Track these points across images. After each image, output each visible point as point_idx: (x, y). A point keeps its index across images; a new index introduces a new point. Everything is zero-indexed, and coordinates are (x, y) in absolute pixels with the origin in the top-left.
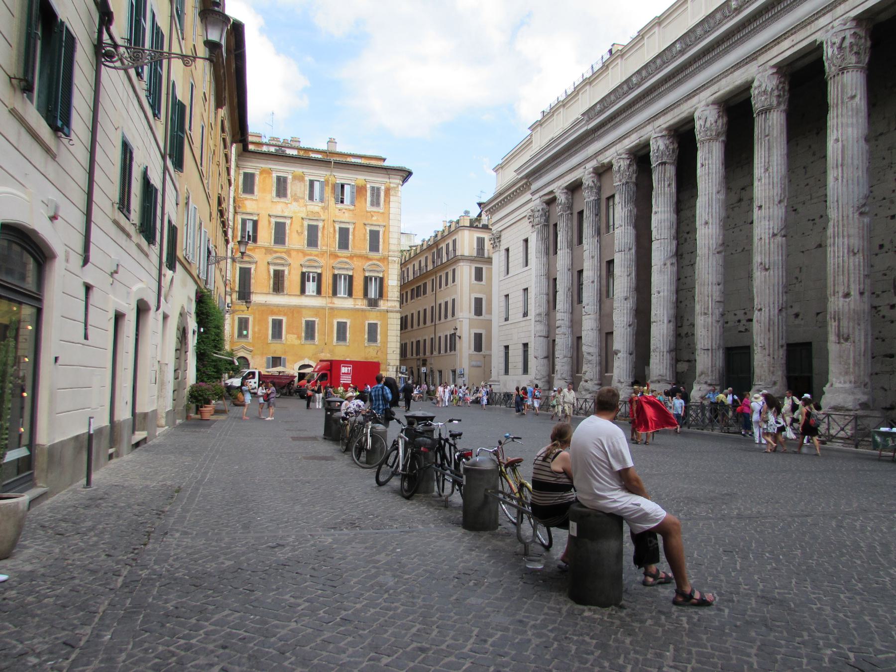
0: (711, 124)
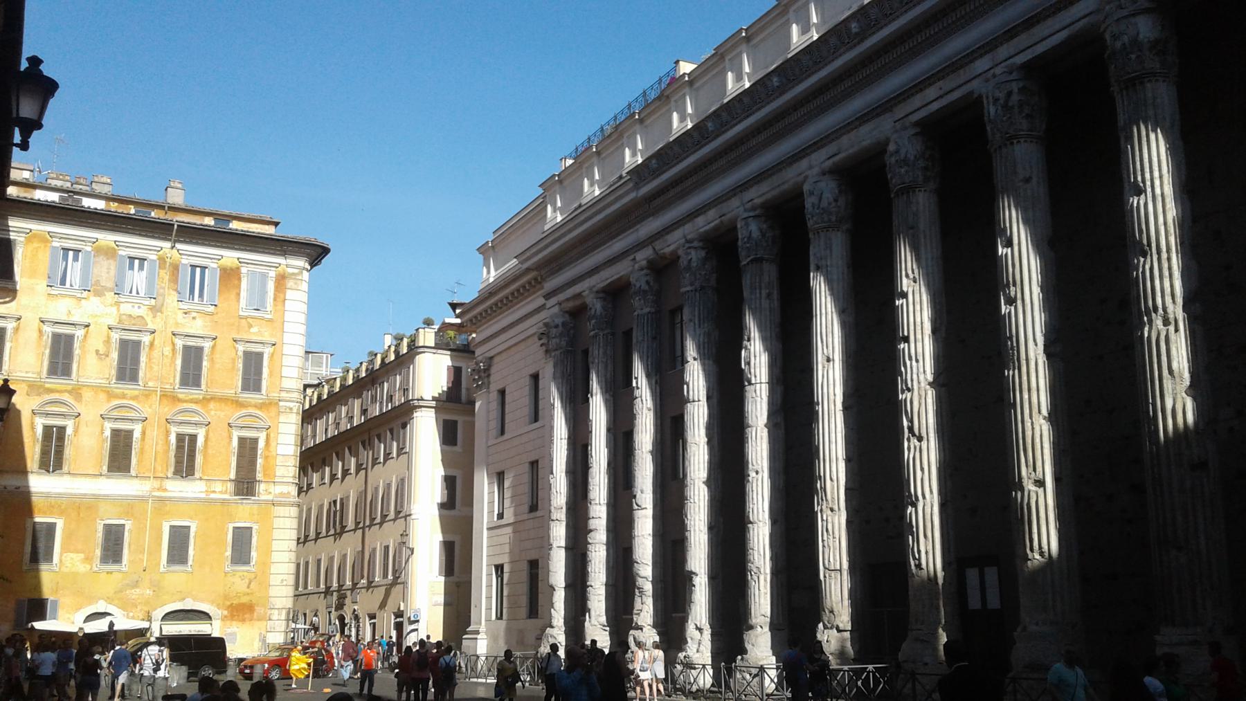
0: (830, 204)
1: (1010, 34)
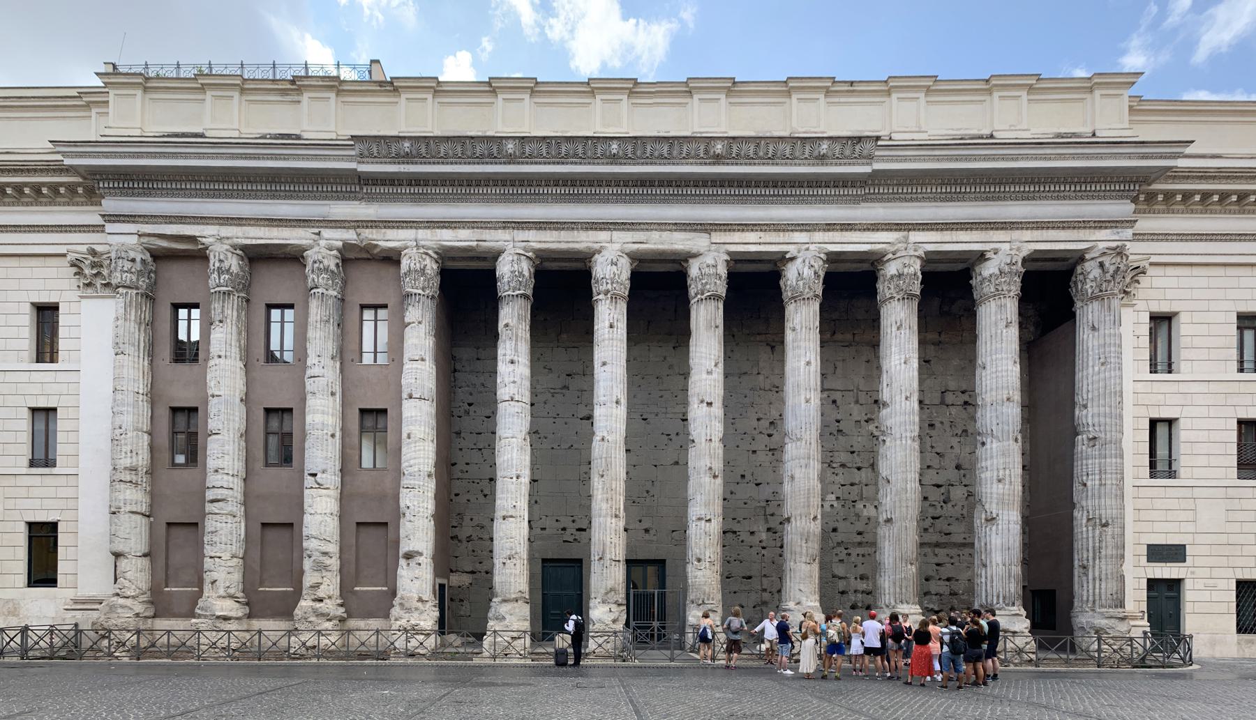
1: (830, 227)
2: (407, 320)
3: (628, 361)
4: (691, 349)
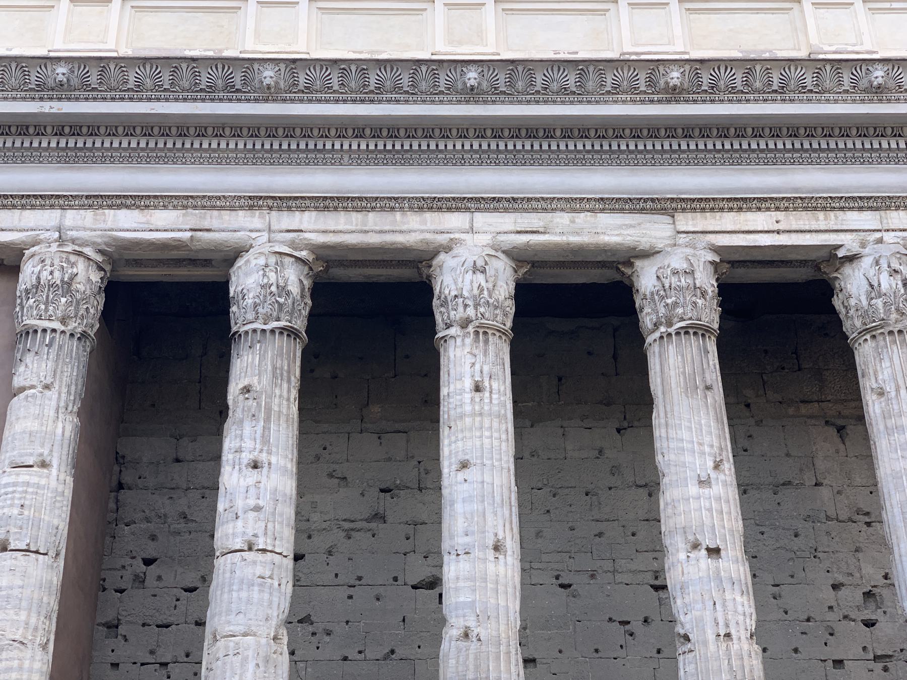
0: (506, 299)
2: (17, 382)
3: (518, 458)
4: (656, 433)
